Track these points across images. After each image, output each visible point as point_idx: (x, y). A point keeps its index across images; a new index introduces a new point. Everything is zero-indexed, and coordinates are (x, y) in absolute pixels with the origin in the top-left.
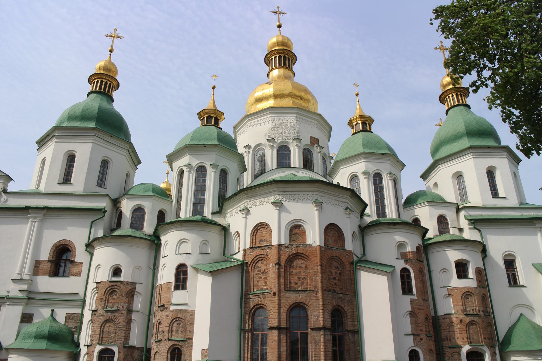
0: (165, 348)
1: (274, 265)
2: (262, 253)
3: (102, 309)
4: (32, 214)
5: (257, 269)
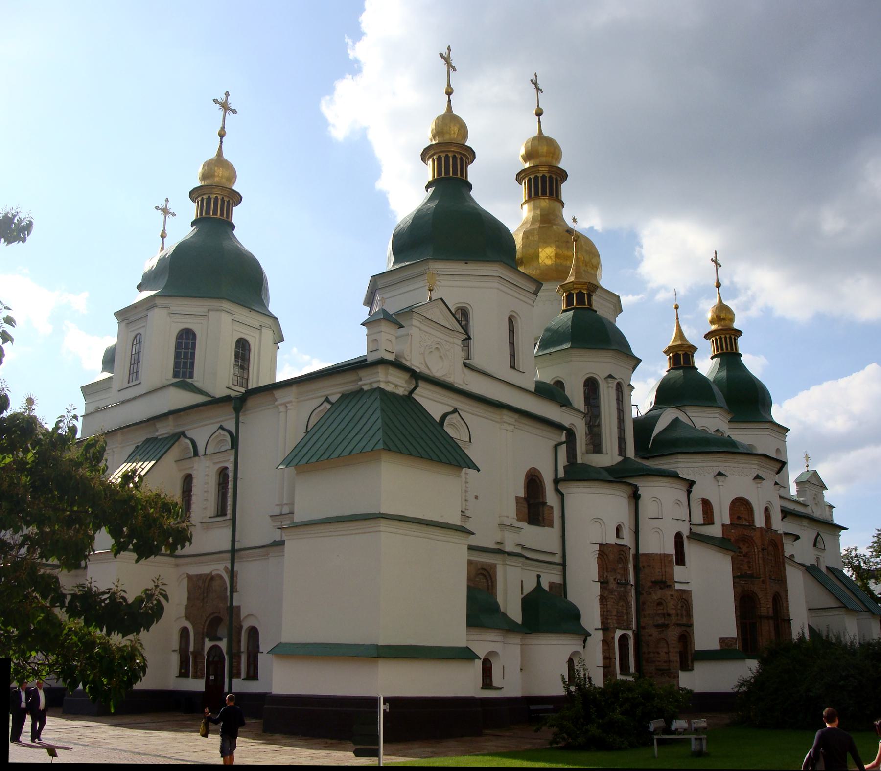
0: (674, 635)
1: (760, 549)
2: (746, 534)
3: (614, 582)
4: (507, 416)
5: (738, 550)
